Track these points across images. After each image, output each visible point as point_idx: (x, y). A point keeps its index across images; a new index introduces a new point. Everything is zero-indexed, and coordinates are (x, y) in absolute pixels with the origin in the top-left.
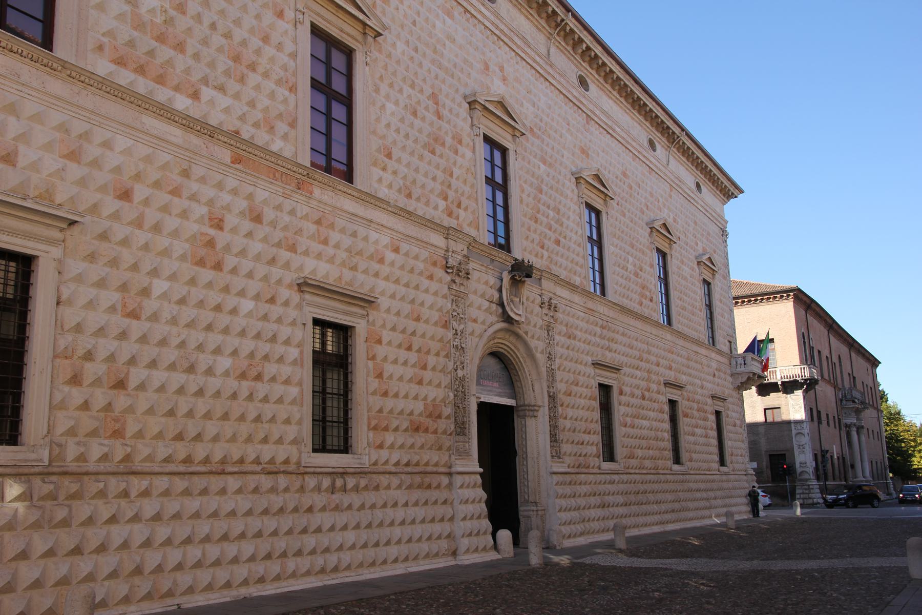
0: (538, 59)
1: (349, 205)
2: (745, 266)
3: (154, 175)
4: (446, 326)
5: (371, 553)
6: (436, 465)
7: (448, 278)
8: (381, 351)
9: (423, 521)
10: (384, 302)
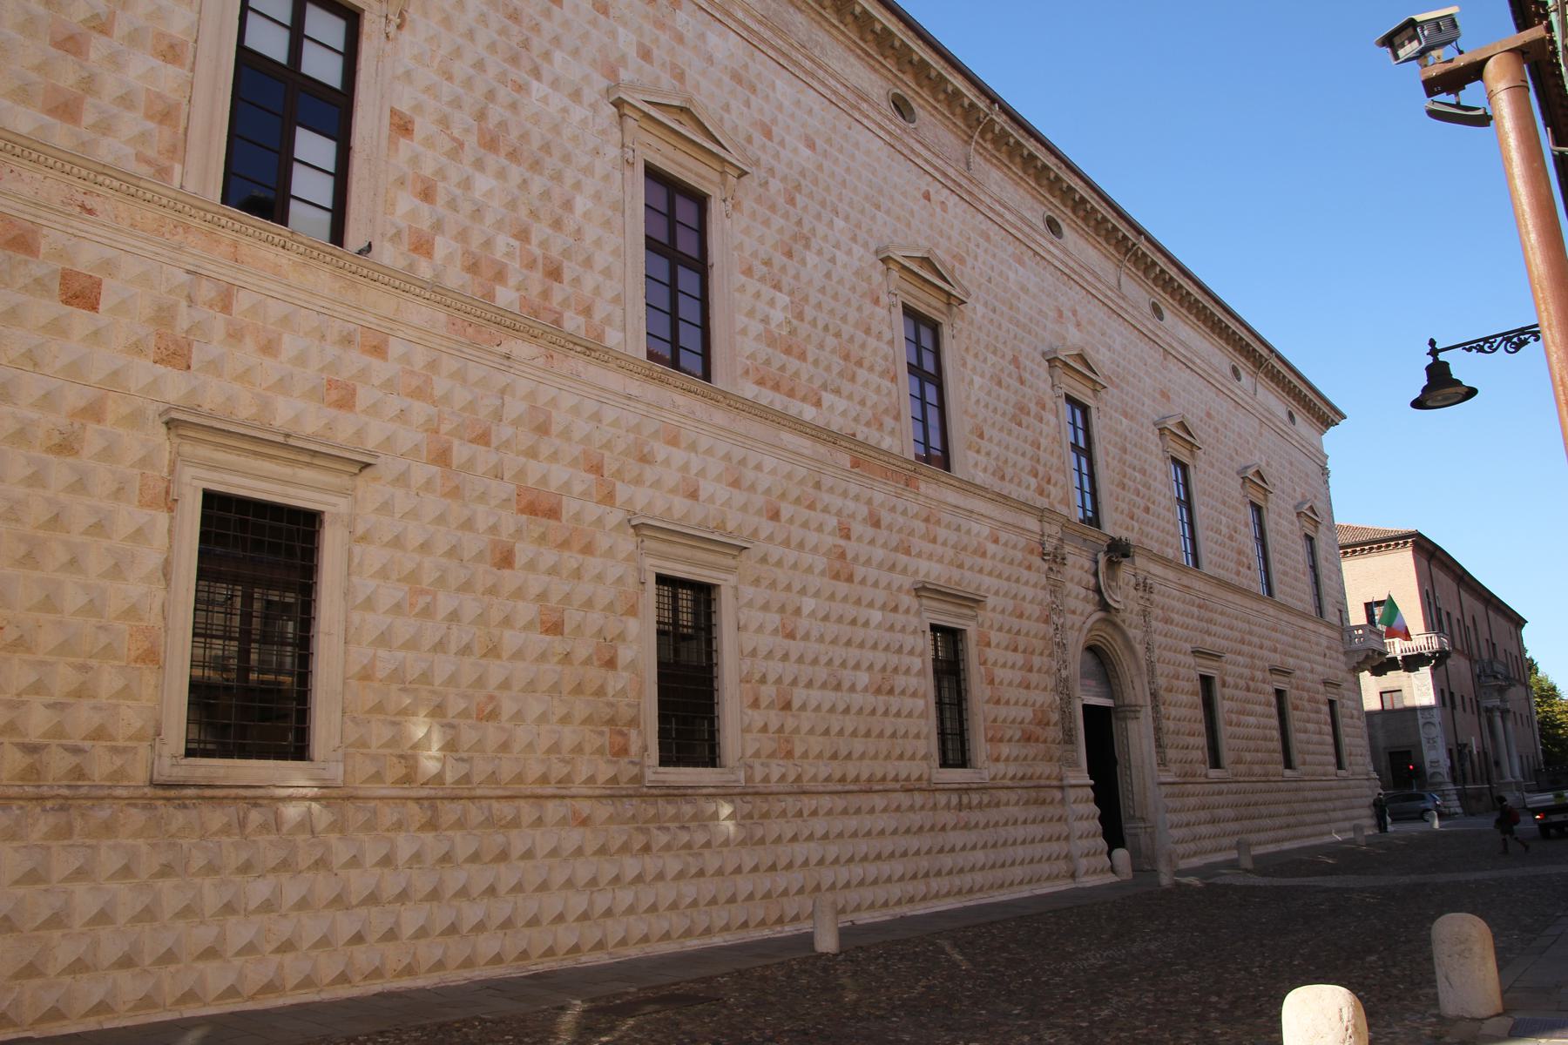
0: (1109, 293)
1: (952, 497)
2: (1352, 508)
3: (795, 492)
4: (1047, 620)
5: (999, 873)
6: (1048, 778)
7: (1046, 566)
8: (992, 654)
9: (1042, 840)
10: (991, 601)
